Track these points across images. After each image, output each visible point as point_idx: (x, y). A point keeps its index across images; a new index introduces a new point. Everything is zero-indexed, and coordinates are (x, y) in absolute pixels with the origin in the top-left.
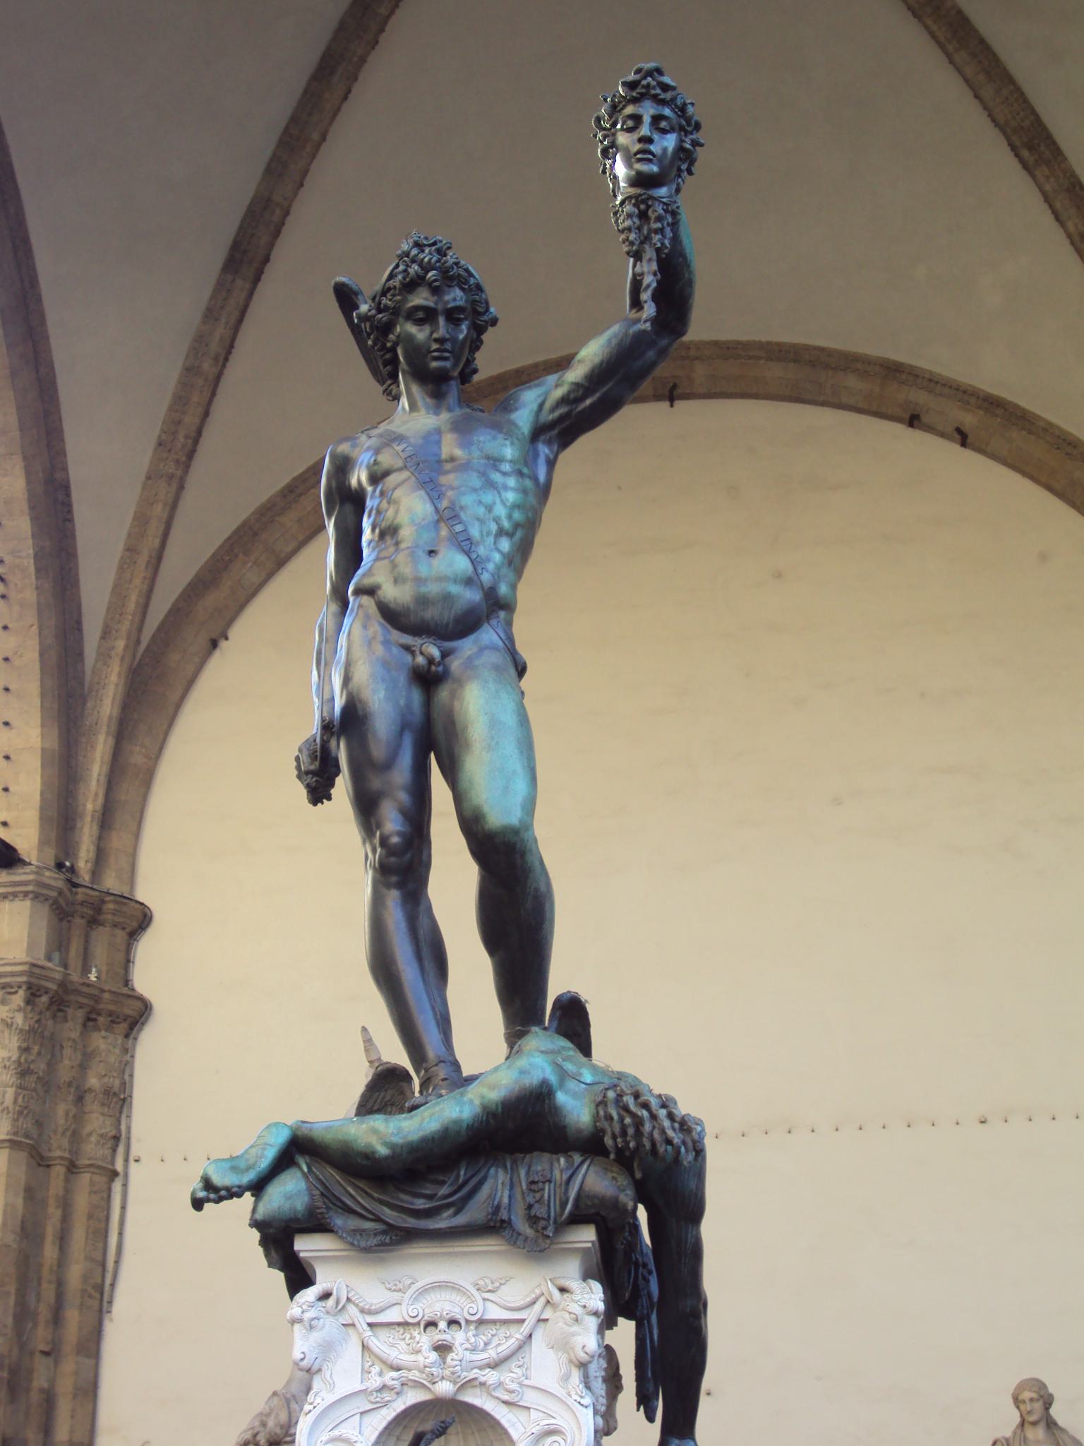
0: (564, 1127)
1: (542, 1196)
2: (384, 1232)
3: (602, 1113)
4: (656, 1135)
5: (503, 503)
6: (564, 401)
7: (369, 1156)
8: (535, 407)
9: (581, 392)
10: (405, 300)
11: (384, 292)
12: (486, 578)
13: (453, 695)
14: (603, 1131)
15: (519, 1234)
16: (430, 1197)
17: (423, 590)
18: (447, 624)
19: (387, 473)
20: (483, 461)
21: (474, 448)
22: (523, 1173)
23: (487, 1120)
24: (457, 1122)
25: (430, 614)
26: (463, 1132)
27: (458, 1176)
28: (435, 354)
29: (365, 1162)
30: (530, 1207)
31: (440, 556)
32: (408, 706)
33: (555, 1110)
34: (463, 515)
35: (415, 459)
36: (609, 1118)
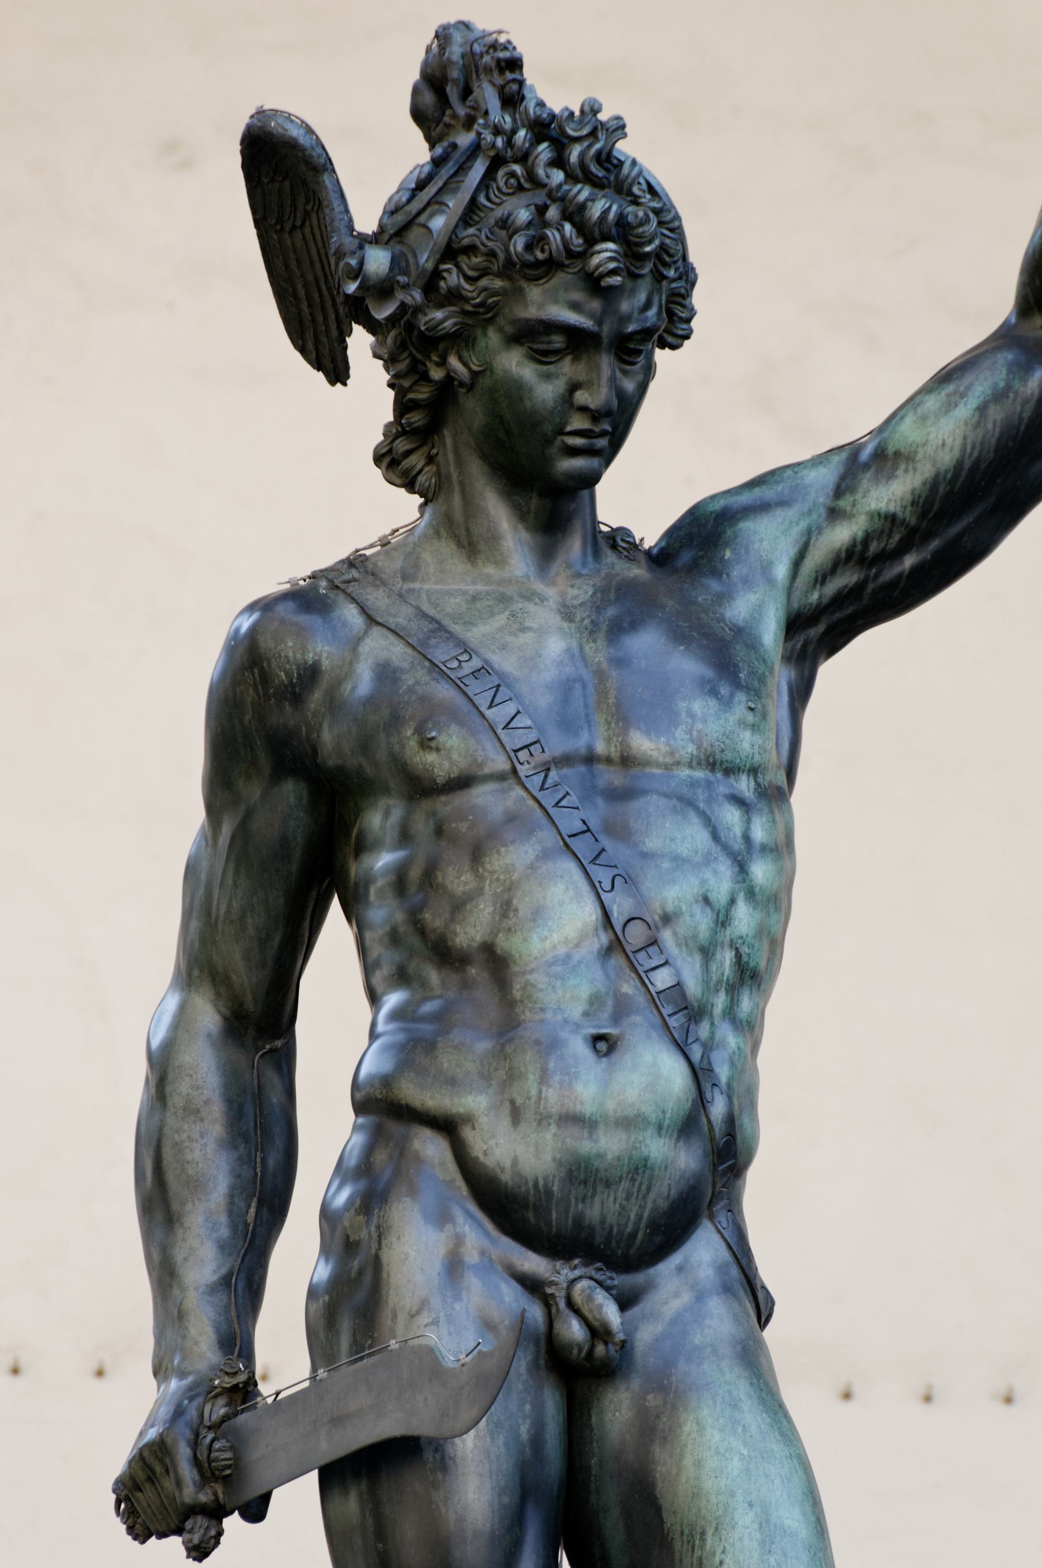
5: (751, 894)
6: (852, 555)
8: (781, 571)
9: (897, 537)
10: (519, 292)
11: (451, 252)
12: (718, 1109)
13: (653, 1429)
17: (586, 1147)
18: (634, 1235)
19: (463, 782)
20: (700, 774)
21: (680, 733)
25: (602, 1210)
28: (578, 441)
31: (624, 1058)
32: (537, 1441)
34: (667, 936)
35: (539, 757)
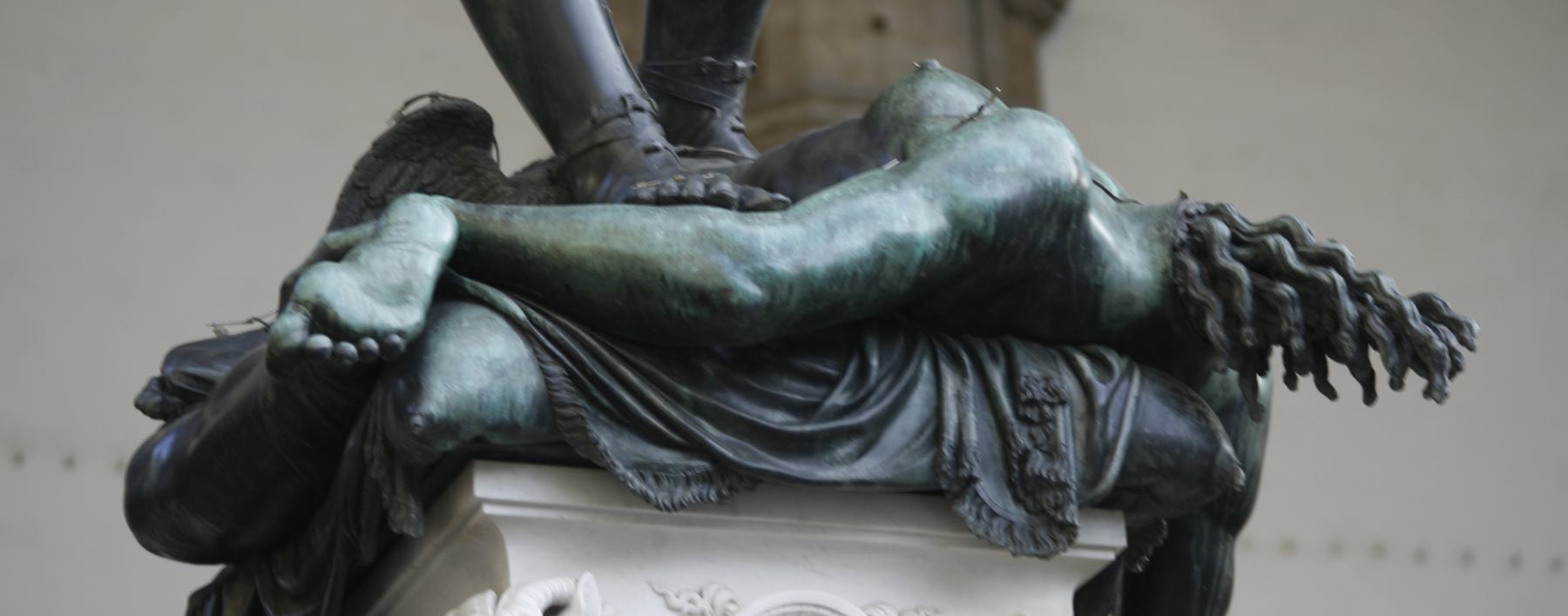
0: (1100, 288)
1: (1051, 436)
2: (706, 478)
3: (1193, 266)
4: (1376, 325)
7: (711, 302)
14: (1202, 308)
15: (993, 514)
16: (805, 411)
22: (997, 377)
23: (958, 252)
24: (905, 245)
26: (911, 271)
27: (864, 370)
29: (691, 311)
30: (1025, 457)
33: (1087, 245)
36: (1219, 279)
